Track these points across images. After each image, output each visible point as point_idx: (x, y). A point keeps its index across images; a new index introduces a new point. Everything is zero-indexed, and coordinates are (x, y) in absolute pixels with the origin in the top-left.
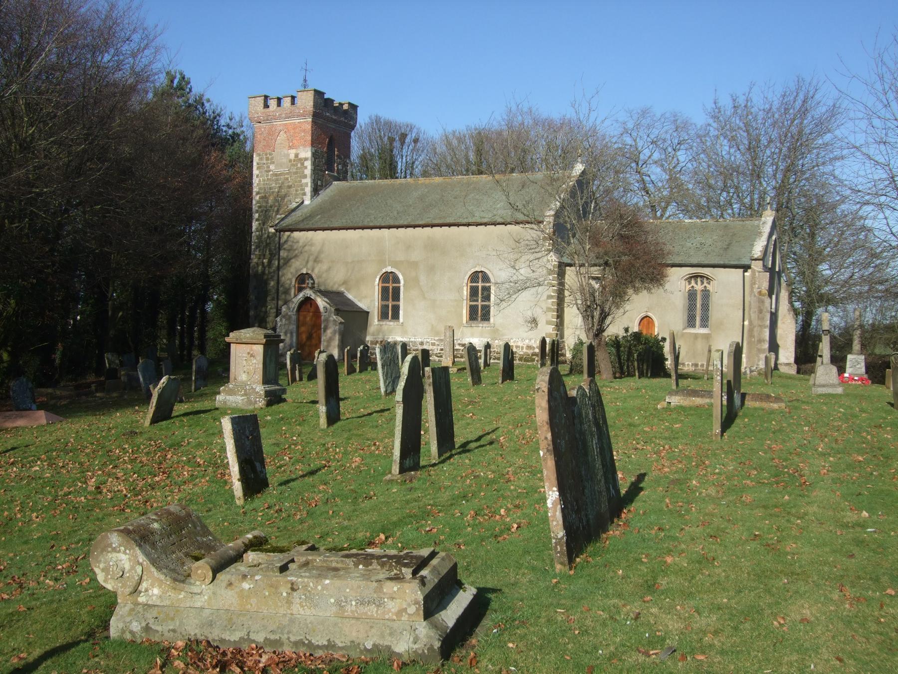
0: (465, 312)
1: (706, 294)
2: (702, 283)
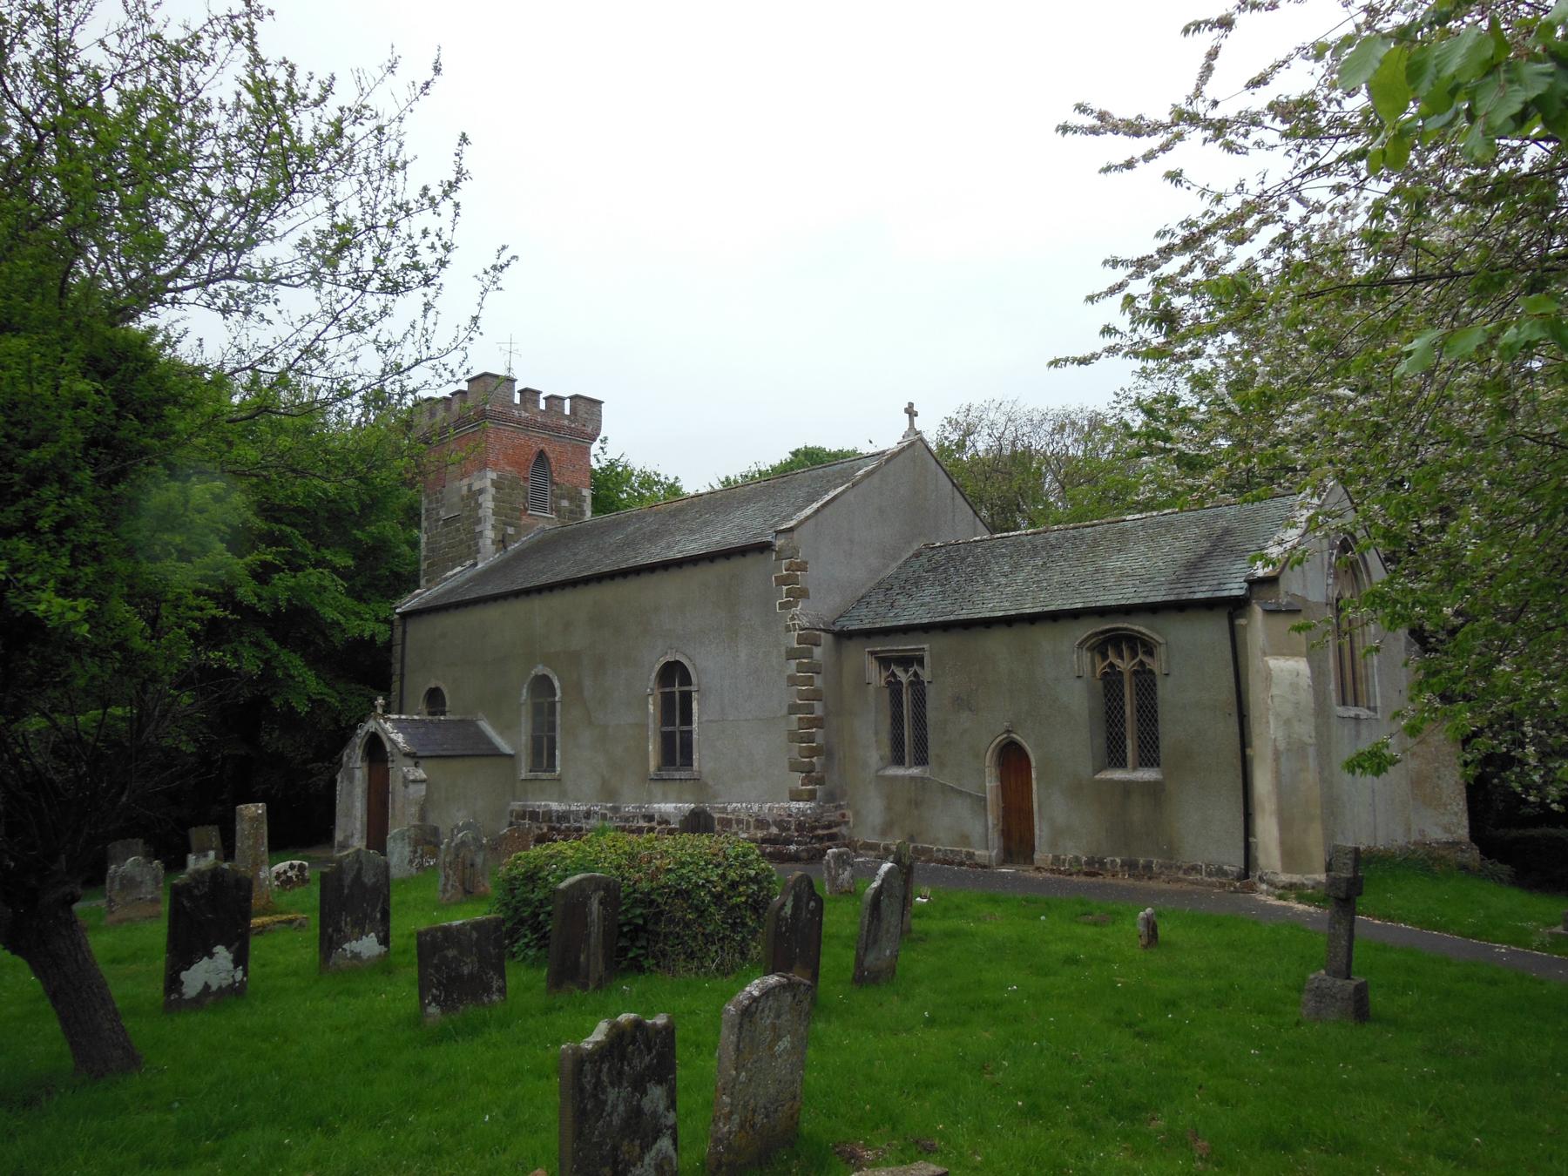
0: (653, 748)
1: (1146, 682)
2: (1134, 655)
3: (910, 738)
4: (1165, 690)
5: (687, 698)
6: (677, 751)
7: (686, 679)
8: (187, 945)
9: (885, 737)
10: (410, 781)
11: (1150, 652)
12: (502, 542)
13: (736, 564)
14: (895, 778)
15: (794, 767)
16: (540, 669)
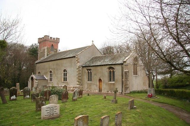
0: (63, 79)
1: (114, 72)
3: (90, 79)
4: (115, 73)
5: (66, 73)
6: (65, 79)
7: (66, 72)
8: (11, 95)
9: (88, 78)
10: (36, 82)
11: (114, 69)
12: (47, 55)
13: (72, 58)
14: (88, 83)
15: (77, 81)
16: (51, 70)
